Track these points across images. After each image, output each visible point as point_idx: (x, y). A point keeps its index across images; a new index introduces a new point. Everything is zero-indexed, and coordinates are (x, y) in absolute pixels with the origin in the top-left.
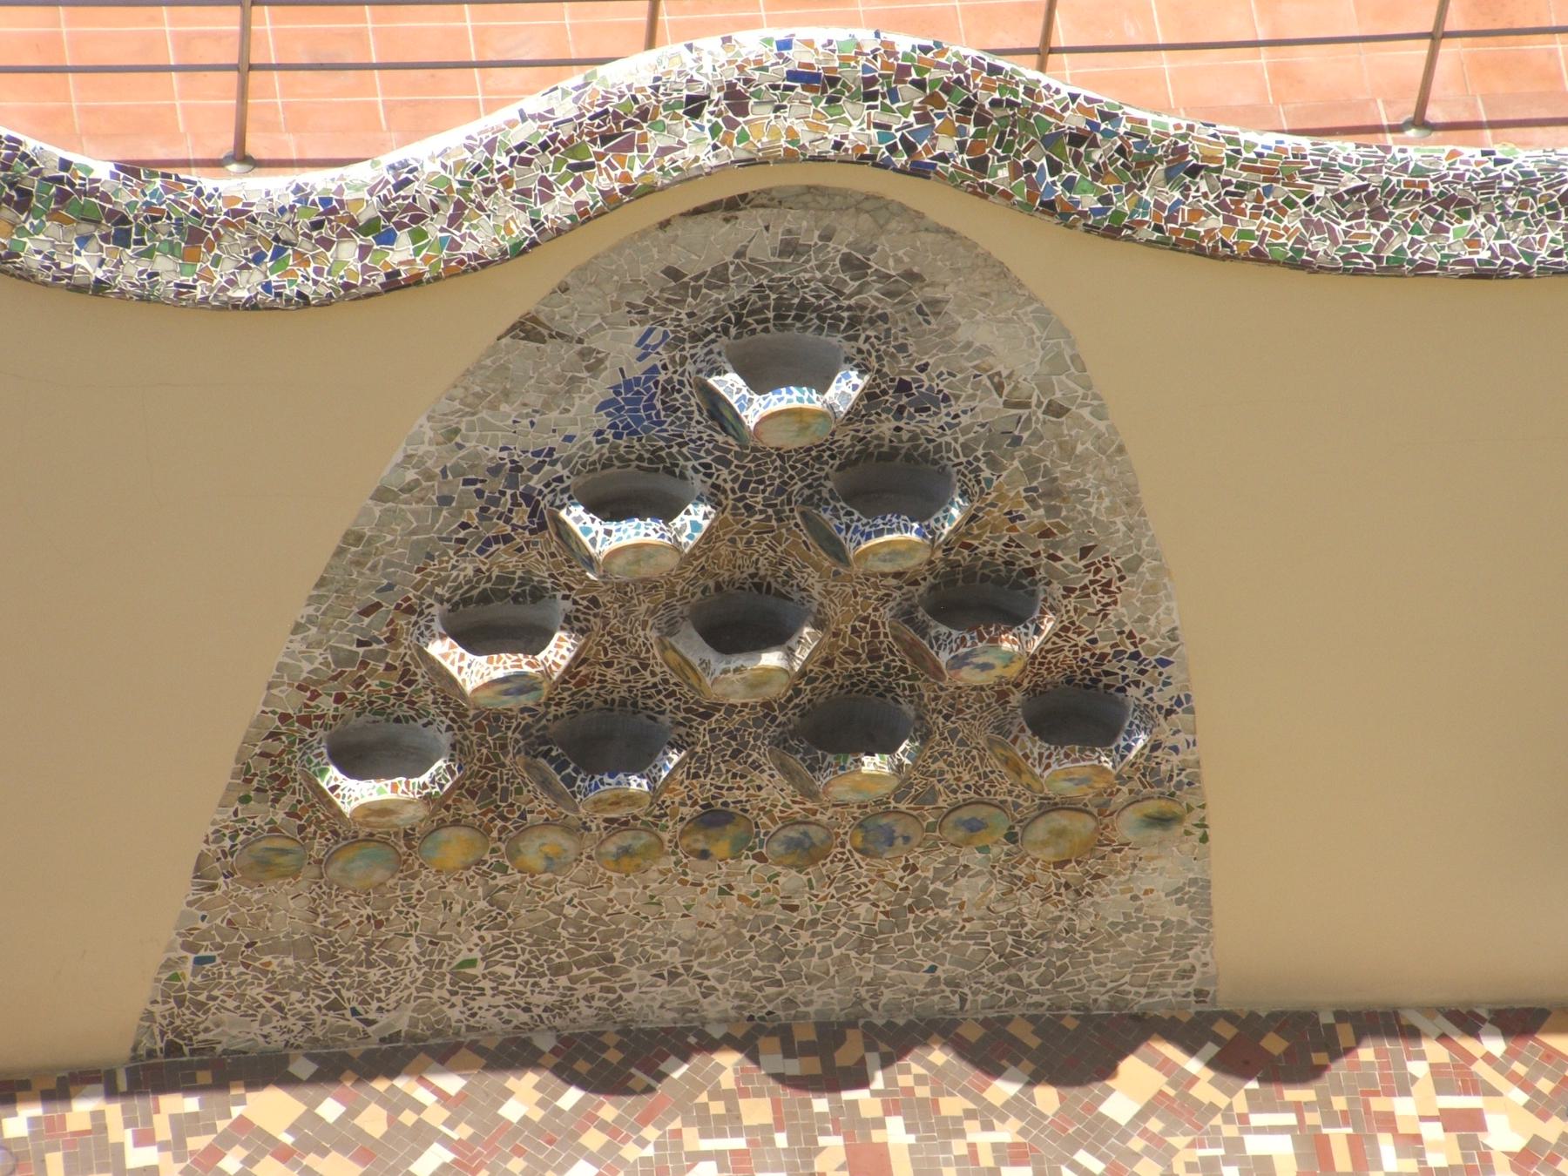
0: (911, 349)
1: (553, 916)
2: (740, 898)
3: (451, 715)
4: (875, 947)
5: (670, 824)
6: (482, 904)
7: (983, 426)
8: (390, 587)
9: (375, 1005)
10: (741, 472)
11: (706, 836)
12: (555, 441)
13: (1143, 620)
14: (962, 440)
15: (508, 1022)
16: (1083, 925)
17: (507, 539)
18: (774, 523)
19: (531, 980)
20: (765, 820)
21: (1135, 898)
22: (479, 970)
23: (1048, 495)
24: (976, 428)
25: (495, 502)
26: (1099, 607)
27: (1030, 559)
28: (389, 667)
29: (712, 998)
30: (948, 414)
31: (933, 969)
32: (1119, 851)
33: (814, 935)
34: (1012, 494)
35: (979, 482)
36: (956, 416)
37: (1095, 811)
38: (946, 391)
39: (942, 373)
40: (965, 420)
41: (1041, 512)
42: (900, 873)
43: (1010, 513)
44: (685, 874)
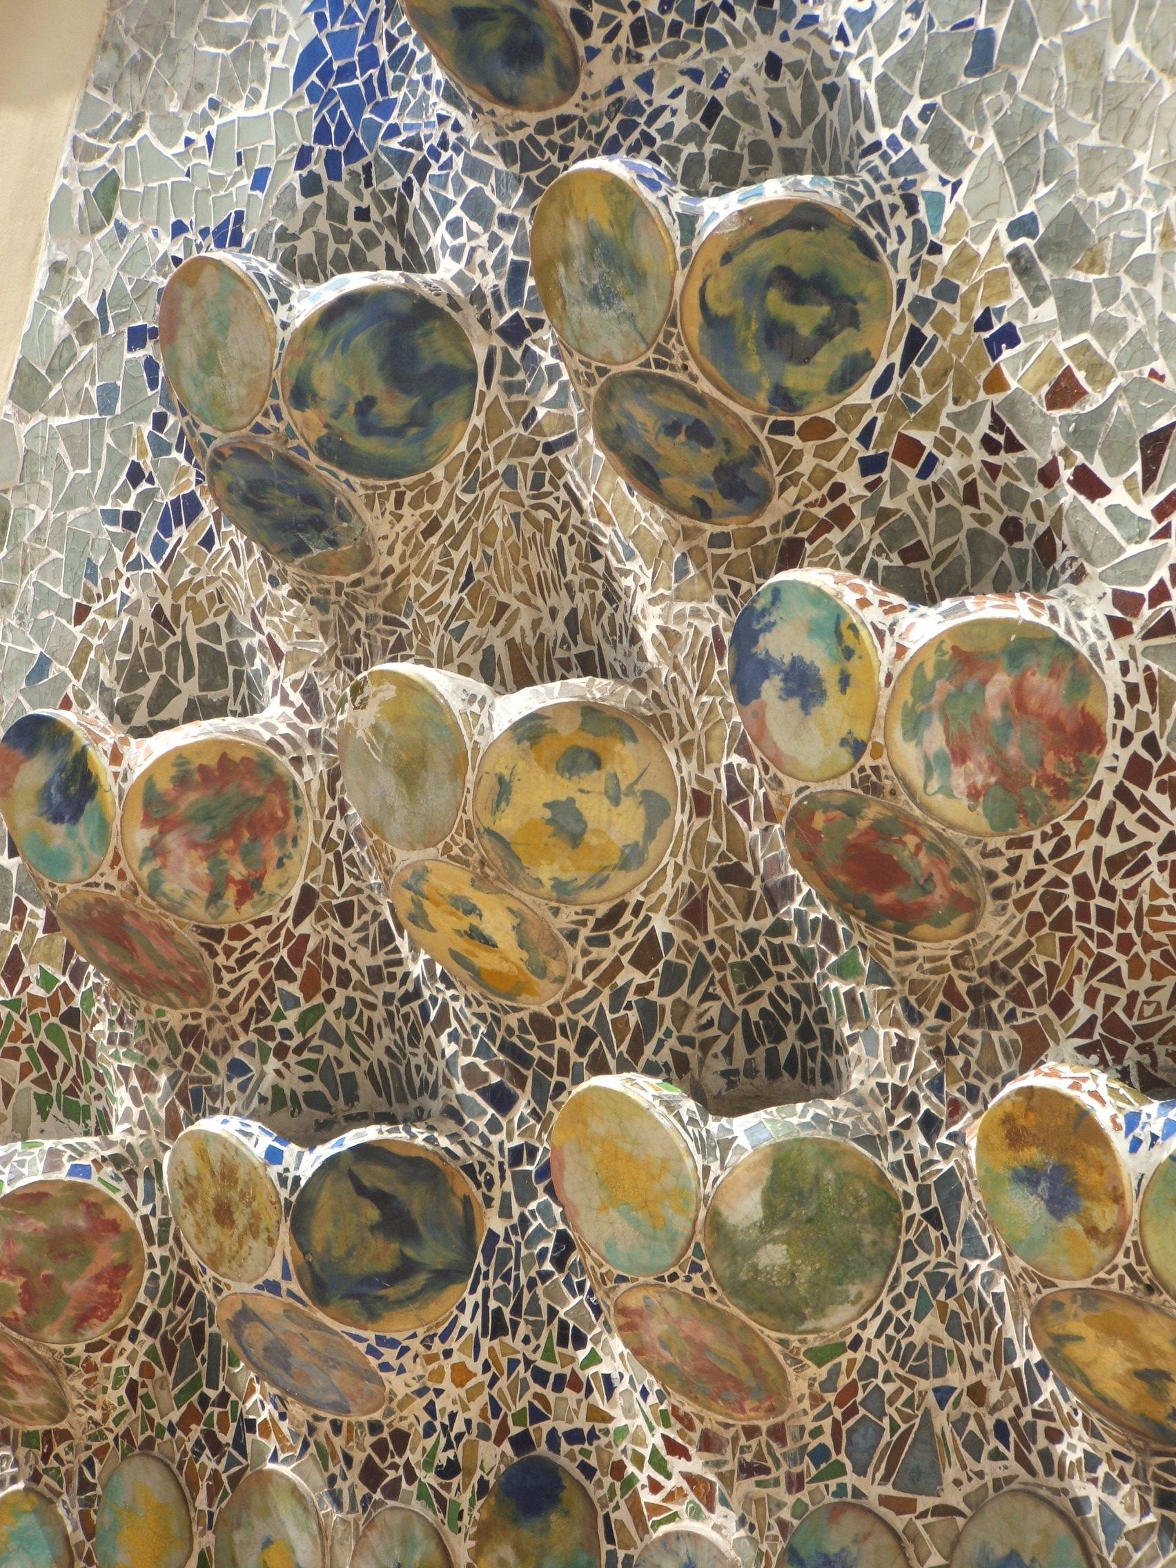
3: (134, 1082)
5: (464, 1499)
14: (877, 70)
27: (1038, 492)
34: (983, 248)
41: (1048, 310)
43: (984, 323)
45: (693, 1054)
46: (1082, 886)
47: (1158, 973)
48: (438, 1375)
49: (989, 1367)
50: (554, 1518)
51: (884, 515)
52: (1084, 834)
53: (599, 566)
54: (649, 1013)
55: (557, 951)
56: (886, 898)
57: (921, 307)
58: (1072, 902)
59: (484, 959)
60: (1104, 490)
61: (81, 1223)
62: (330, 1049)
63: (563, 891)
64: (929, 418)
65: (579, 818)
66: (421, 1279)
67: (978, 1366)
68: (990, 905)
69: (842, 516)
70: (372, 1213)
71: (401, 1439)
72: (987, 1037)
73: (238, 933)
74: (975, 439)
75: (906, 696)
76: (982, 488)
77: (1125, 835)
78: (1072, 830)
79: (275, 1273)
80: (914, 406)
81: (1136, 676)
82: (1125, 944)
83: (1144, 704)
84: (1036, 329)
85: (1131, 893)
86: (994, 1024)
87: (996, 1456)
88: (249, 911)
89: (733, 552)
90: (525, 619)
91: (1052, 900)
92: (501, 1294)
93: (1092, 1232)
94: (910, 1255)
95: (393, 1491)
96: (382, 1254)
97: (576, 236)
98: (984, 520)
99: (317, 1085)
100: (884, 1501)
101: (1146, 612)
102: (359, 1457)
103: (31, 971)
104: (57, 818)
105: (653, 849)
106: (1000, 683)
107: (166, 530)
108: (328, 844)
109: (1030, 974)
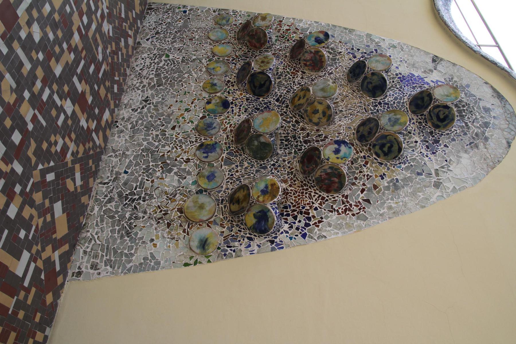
0: (454, 142)
1: (184, 72)
2: (182, 114)
4: (145, 154)
5: (225, 95)
6: (194, 57)
7: (425, 164)
10: (392, 103)
11: (217, 103)
13: (330, 225)
14: (417, 158)
16: (140, 223)
18: (370, 112)
19: (155, 70)
20: (222, 118)
21: (152, 240)
23: (394, 184)
24: (423, 162)
26: (336, 209)
27: (361, 183)
29: (131, 111)
30: (427, 154)
32: (184, 231)
33: (157, 136)
34: (394, 174)
35: (400, 163)
36: (427, 156)
37: (212, 220)
38: (437, 153)
39: (445, 151)
40: (426, 159)
41: (386, 185)
42: (185, 158)
43: (384, 174)
44: (198, 100)
45: (283, 128)
46: (307, 189)
47: (295, 200)
48: (241, 91)
49: (241, 173)
50: (222, 108)
51: (358, 159)
52: (314, 190)
53: (349, 115)
54: (289, 122)
55: (298, 109)
56: (305, 160)
57: (386, 165)
58: (305, 188)
59: (297, 99)
60: (362, 193)
61: (262, 42)
62: (284, 75)
63: (306, 111)
64: (371, 166)
65: (315, 114)
66: (254, 89)
67: (241, 172)
68: (305, 176)
69: (357, 152)
70: (262, 83)
71: (233, 86)
72: (286, 174)
73: (300, 63)
74: (368, 173)
75: (335, 167)
76: (362, 174)
77: (314, 196)
78: (315, 188)
79: (255, 69)
80: (373, 164)
81: (336, 198)
82: (299, 196)
83: (333, 199)
84: (384, 182)
85: (306, 197)
86: (288, 175)
87: (229, 174)
88: (302, 65)
89: (352, 136)
90: (342, 104)
91: (305, 185)
92: (252, 100)
93: (258, 197)
94: (256, 162)
95: (227, 85)
96: (257, 84)
98: (357, 174)
99: (279, 74)
100: (223, 157)
101: (345, 200)
102: (231, 80)
103: (294, 35)
104: (315, 39)
105: (311, 123)
106: (336, 180)
107: (352, 54)
108: (311, 76)
109: (295, 181)
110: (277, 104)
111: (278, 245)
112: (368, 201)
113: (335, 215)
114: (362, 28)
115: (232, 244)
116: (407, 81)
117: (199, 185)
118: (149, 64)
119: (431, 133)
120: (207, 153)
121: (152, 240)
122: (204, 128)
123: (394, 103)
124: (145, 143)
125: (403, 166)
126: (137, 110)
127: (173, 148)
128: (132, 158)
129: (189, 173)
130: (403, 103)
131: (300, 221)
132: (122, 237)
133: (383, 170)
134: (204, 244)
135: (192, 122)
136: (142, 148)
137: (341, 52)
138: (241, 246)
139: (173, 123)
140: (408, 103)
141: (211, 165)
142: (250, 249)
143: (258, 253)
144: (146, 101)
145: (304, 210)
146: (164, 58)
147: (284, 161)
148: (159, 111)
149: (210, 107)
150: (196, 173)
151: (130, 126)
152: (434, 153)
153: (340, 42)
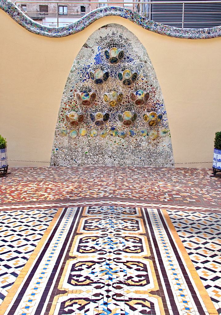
0: (128, 51)
6: (87, 142)
8: (73, 87)
9: (77, 159)
12: (90, 64)
15: (92, 163)
16: (158, 151)
17: (86, 80)
21: (163, 147)
22: (88, 154)
25: (84, 74)
28: (74, 101)
31: (141, 158)
32: (160, 138)
33: (126, 151)
40: (135, 63)
42: (135, 141)
54: (121, 108)
57: (138, 77)
69: (134, 86)
71: (103, 127)
95: (103, 129)
97: (126, 73)
102: (100, 128)
110: (112, 111)
111: (165, 113)
112: (151, 85)
113: (156, 96)
114: (68, 74)
115: (164, 125)
116: (99, 62)
117: (146, 135)
118: (91, 159)
119: (125, 59)
120: (134, 134)
121: (163, 147)
122: (124, 135)
123: (111, 69)
124: (129, 154)
125: (139, 72)
126: (115, 159)
127: (132, 145)
128: (135, 157)
129: (141, 139)
130: (111, 66)
131: (158, 106)
132: (162, 155)
133: (140, 79)
134: (165, 132)
135: (121, 140)
136: (131, 155)
137: (83, 85)
138: (165, 123)
139: (121, 146)
140: (111, 64)
141: (138, 132)
142: (166, 120)
143: (167, 118)
144: (111, 157)
145: (154, 105)
146: (88, 154)
147: (137, 110)
148: (115, 152)
149: (114, 134)
150: (141, 137)
151: (122, 160)
152: (133, 60)
153: (76, 84)
